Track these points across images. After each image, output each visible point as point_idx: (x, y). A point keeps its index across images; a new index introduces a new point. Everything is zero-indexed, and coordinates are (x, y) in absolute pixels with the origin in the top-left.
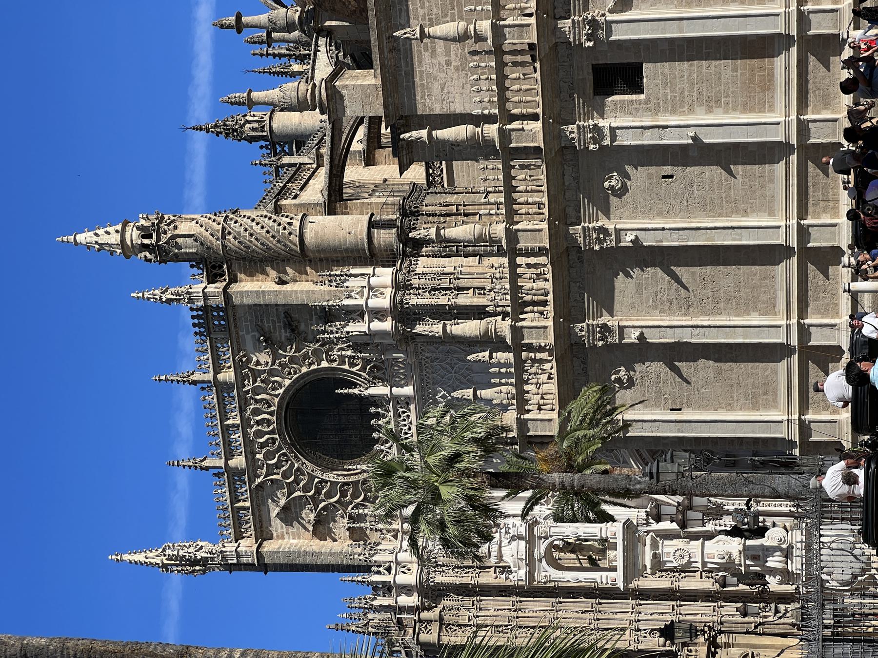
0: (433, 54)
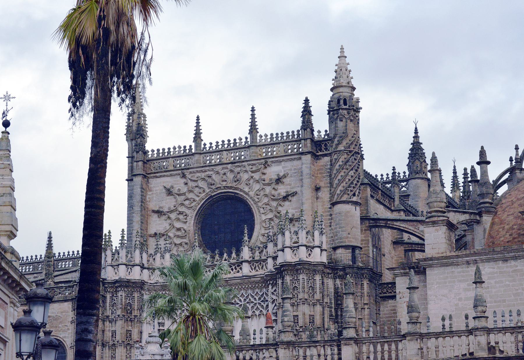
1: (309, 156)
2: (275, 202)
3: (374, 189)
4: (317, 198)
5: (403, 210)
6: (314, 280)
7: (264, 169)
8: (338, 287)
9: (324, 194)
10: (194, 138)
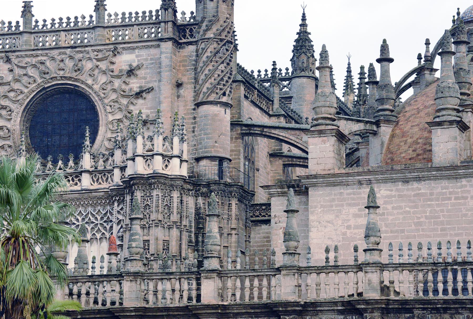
0: (356, 216)
1: (170, 44)
2: (125, 99)
3: (249, 88)
4: (178, 97)
5: (283, 115)
6: (171, 197)
8: (200, 208)
10: (23, 12)
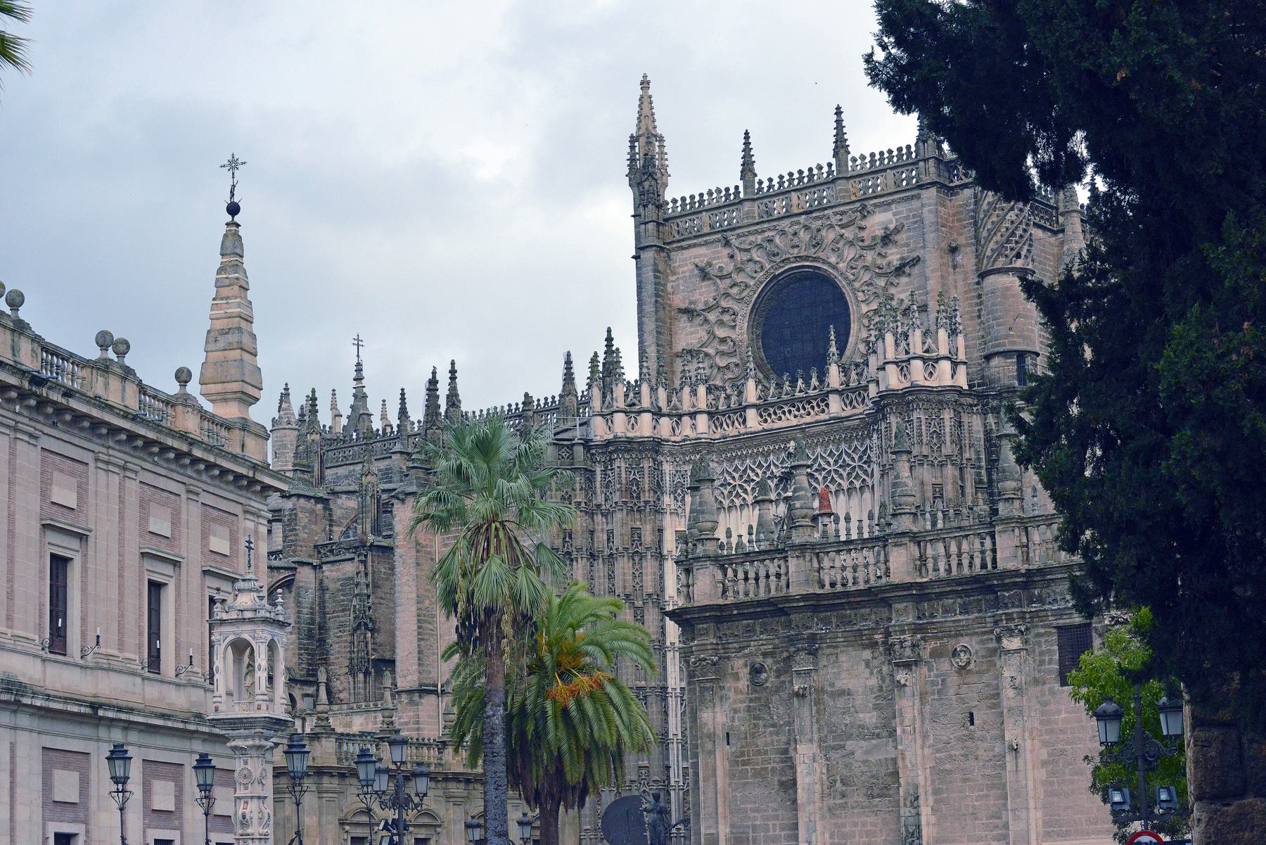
1: (933, 191)
4: (955, 267)
7: (861, 220)
8: (991, 430)
9: (966, 259)
10: (742, 172)
